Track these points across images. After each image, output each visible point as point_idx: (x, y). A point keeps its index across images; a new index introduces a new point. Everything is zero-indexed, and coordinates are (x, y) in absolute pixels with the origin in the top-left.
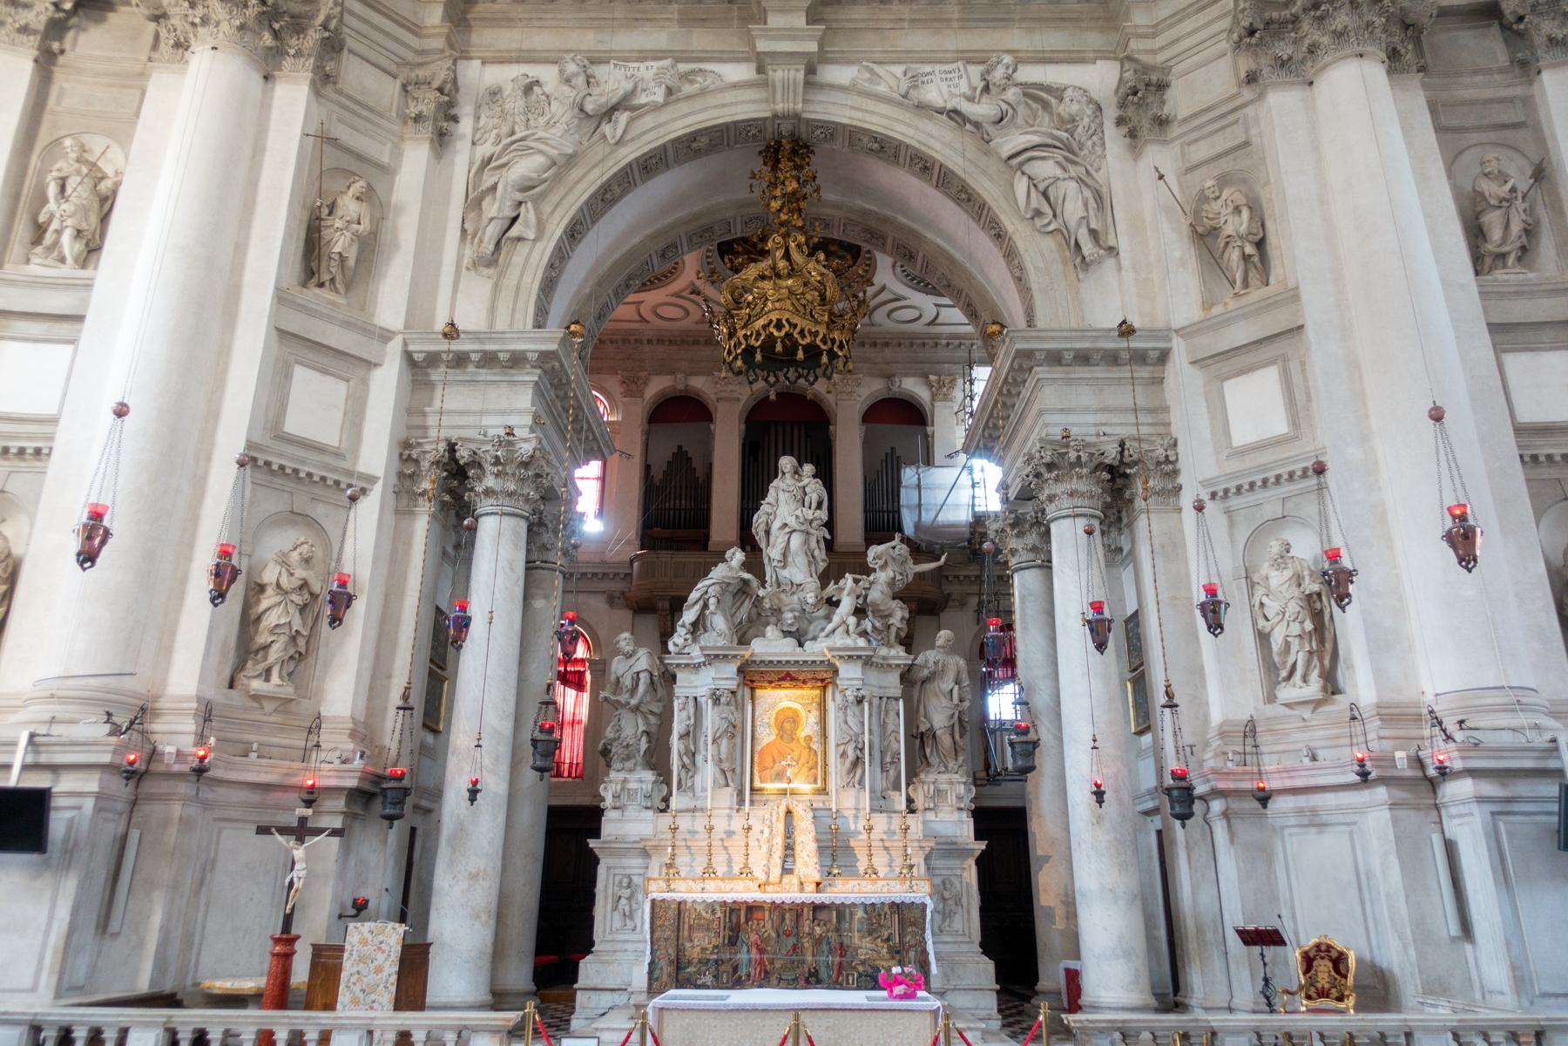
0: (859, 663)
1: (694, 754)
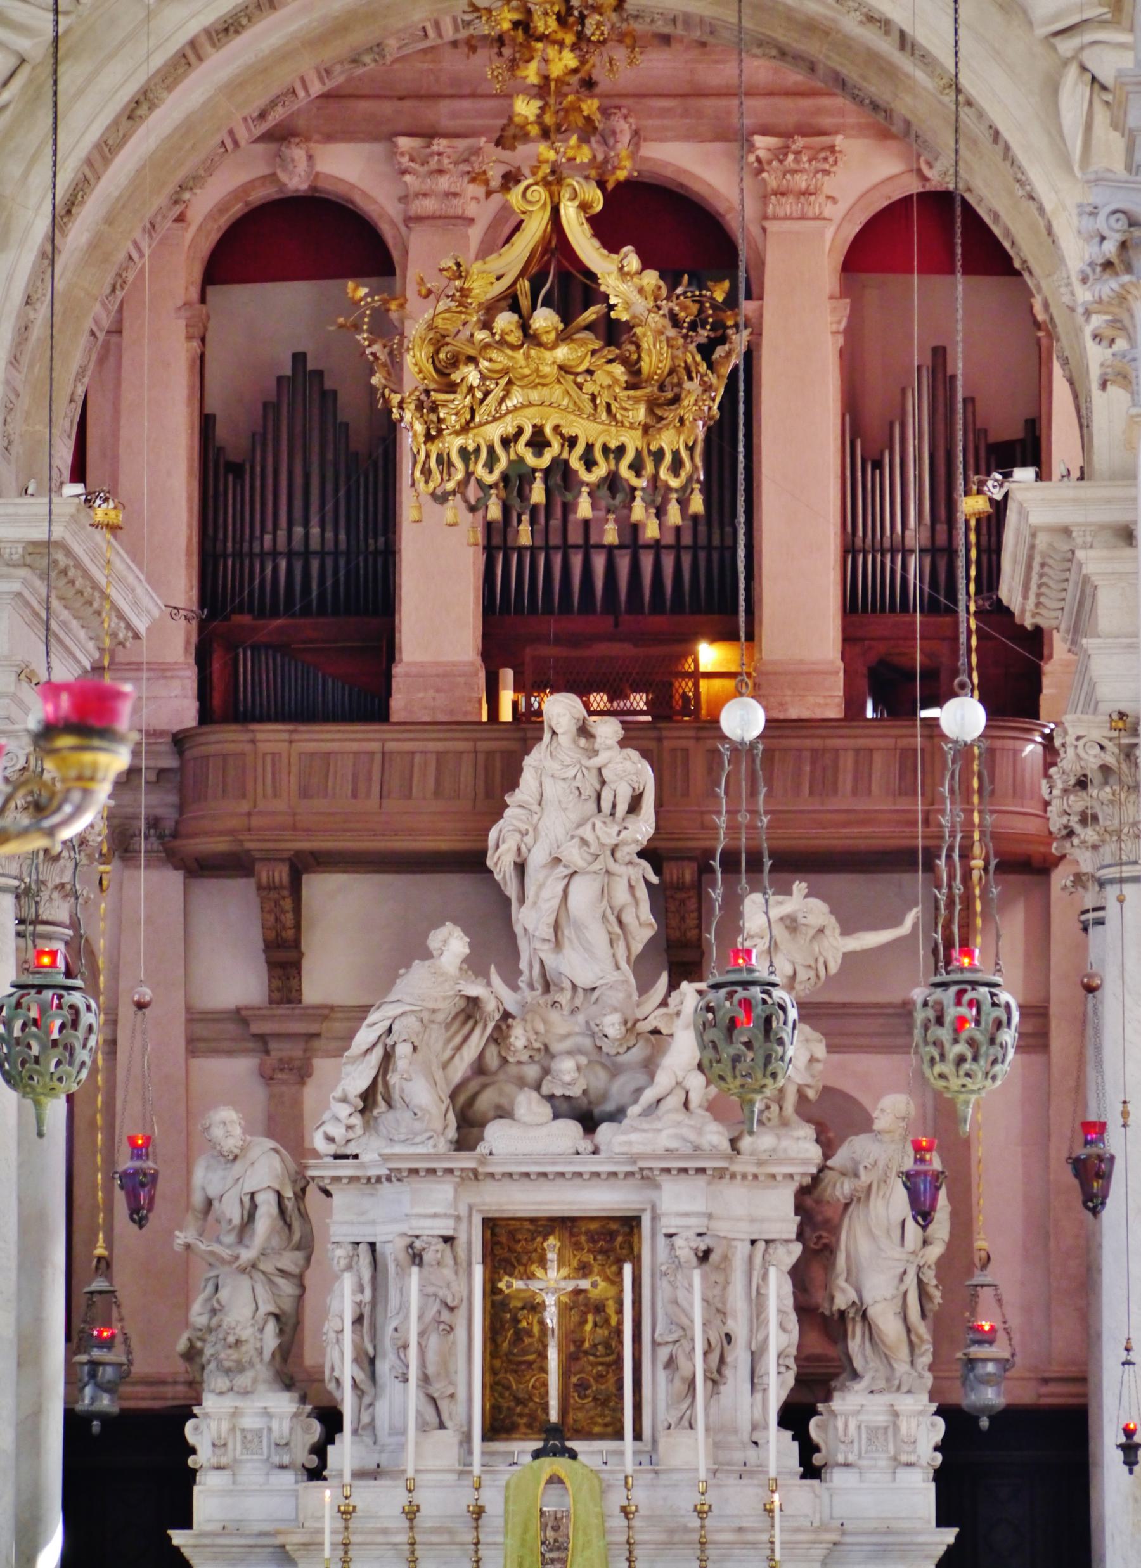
0: (701, 1180)
1: (372, 1361)
